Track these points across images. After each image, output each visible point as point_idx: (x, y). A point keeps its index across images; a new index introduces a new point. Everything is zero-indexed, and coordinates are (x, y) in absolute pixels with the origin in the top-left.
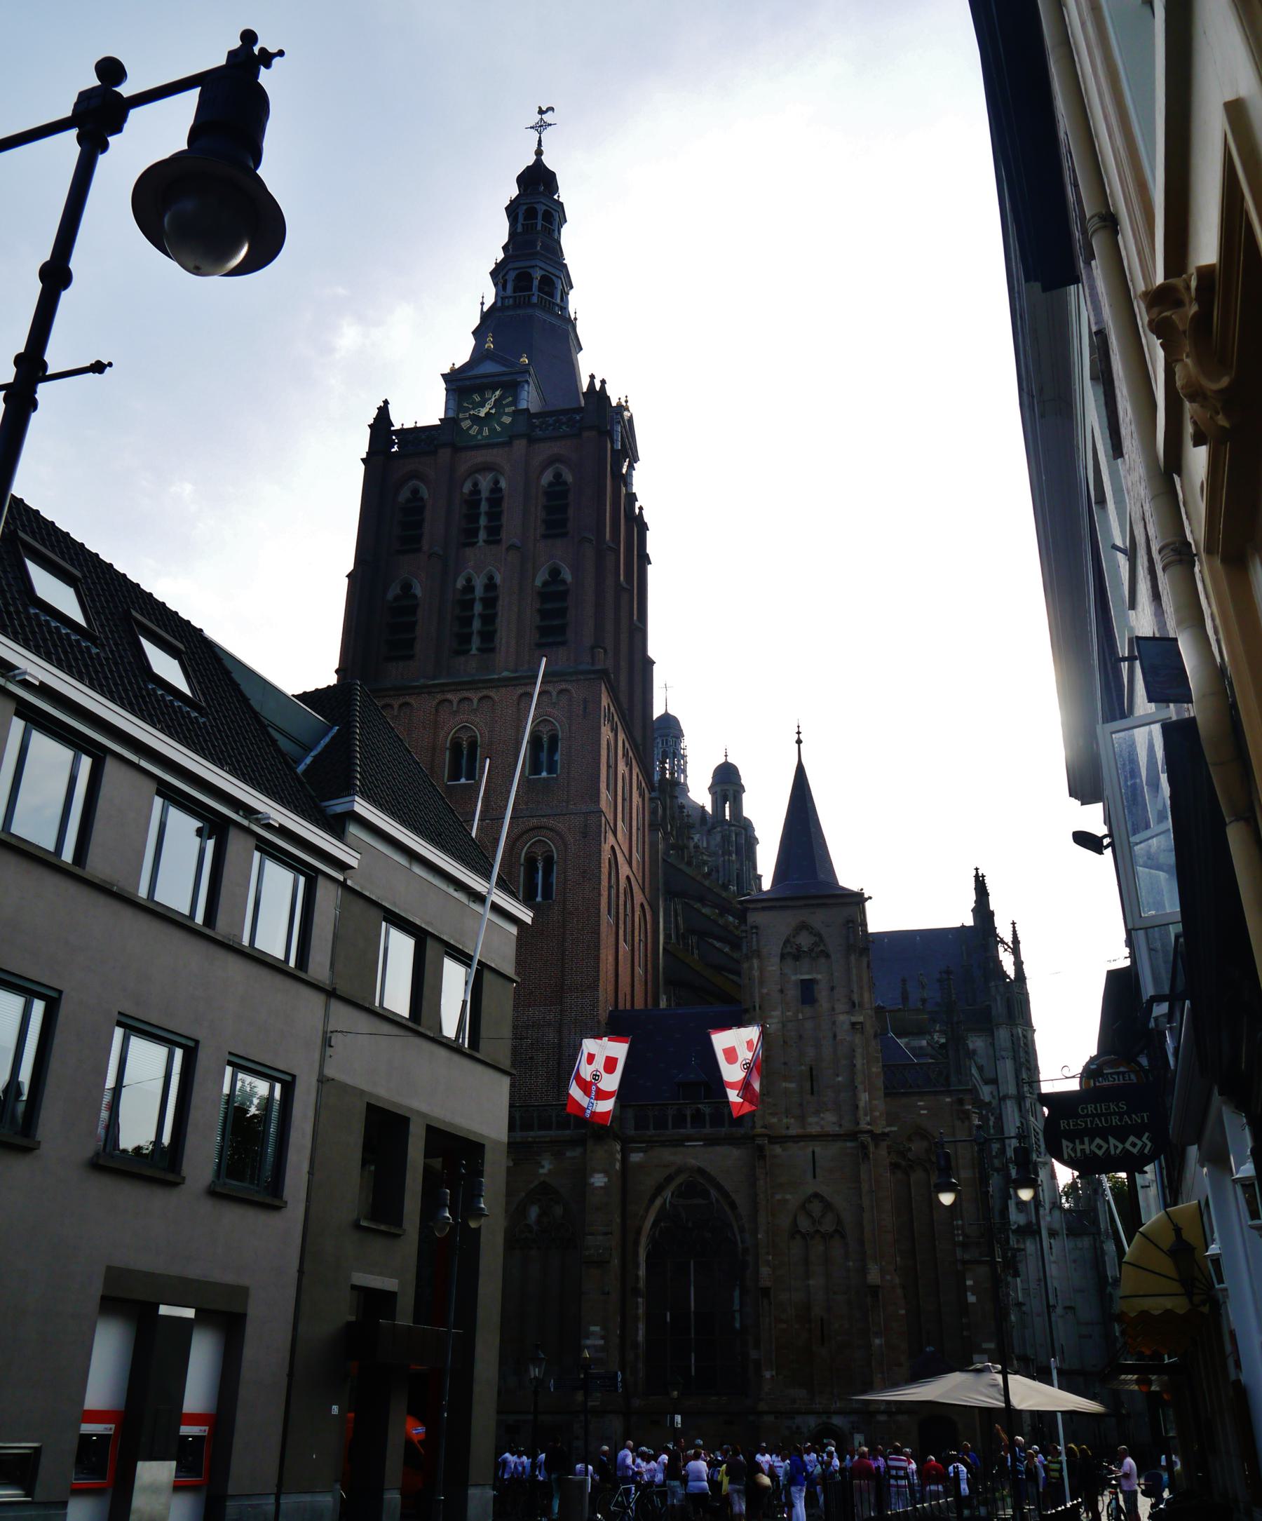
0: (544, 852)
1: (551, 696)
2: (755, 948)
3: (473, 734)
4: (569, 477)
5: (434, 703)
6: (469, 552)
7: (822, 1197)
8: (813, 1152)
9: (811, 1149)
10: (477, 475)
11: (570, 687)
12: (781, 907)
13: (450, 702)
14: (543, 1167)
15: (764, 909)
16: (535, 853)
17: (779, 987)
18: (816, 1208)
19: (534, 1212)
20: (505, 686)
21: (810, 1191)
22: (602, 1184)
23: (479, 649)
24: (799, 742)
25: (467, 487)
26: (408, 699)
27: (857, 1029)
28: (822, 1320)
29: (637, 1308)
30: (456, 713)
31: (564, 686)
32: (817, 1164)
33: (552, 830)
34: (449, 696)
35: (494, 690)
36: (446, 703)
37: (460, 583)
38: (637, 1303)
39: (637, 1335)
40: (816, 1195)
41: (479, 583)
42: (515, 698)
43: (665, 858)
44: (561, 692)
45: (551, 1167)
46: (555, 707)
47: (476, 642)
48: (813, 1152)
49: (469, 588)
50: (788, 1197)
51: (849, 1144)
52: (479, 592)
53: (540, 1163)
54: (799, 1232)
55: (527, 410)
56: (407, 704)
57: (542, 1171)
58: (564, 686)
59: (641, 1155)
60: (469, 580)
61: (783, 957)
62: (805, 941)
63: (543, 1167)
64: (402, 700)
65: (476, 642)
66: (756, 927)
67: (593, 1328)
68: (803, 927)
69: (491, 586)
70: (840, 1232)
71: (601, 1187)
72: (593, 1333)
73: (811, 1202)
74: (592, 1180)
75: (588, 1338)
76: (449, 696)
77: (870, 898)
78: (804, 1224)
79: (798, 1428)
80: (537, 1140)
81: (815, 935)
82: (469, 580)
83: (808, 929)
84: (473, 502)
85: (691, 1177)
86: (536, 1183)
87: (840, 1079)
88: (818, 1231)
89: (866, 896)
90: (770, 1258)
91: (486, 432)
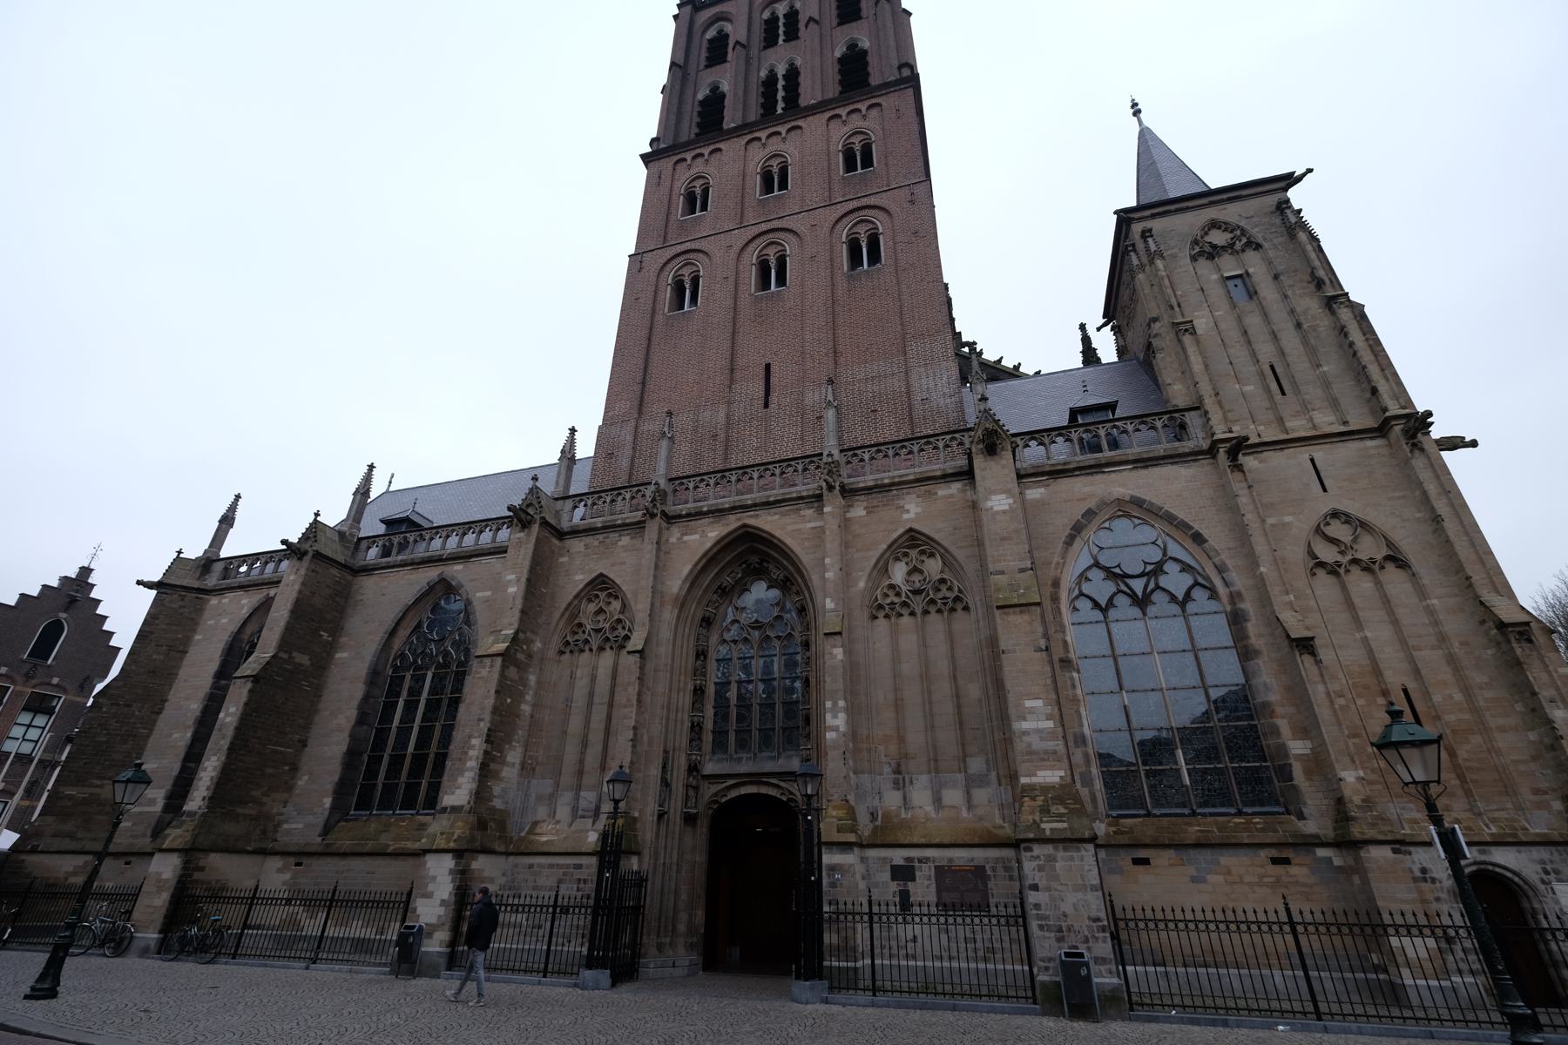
5: (744, 143)
6: (770, 51)
7: (1346, 515)
8: (1312, 460)
9: (1307, 456)
12: (1177, 211)
13: (759, 139)
16: (857, 233)
17: (1197, 286)
18: (1338, 530)
19: (899, 573)
20: (812, 115)
21: (1325, 509)
22: (1007, 507)
23: (784, 41)
24: (1137, 113)
26: (717, 146)
27: (1342, 303)
28: (1405, 691)
29: (1074, 686)
30: (764, 145)
32: (1322, 475)
37: (763, 73)
38: (1072, 679)
40: (1335, 514)
41: (781, 70)
42: (824, 121)
44: (870, 107)
45: (919, 510)
48: (1312, 460)
50: (1288, 519)
54: (1321, 564)
56: (719, 150)
57: (905, 516)
59: (1042, 490)
60: (771, 71)
61: (1194, 258)
62: (1219, 238)
63: (908, 511)
70: (1396, 559)
71: (1004, 512)
72: (1032, 711)
73: (1328, 524)
74: (989, 504)
75: (1025, 719)
78: (1327, 554)
79: (1424, 871)
80: (896, 480)
82: (771, 71)
83: (1219, 228)
85: (1119, 510)
86: (901, 531)
88: (1355, 561)
90: (1292, 597)
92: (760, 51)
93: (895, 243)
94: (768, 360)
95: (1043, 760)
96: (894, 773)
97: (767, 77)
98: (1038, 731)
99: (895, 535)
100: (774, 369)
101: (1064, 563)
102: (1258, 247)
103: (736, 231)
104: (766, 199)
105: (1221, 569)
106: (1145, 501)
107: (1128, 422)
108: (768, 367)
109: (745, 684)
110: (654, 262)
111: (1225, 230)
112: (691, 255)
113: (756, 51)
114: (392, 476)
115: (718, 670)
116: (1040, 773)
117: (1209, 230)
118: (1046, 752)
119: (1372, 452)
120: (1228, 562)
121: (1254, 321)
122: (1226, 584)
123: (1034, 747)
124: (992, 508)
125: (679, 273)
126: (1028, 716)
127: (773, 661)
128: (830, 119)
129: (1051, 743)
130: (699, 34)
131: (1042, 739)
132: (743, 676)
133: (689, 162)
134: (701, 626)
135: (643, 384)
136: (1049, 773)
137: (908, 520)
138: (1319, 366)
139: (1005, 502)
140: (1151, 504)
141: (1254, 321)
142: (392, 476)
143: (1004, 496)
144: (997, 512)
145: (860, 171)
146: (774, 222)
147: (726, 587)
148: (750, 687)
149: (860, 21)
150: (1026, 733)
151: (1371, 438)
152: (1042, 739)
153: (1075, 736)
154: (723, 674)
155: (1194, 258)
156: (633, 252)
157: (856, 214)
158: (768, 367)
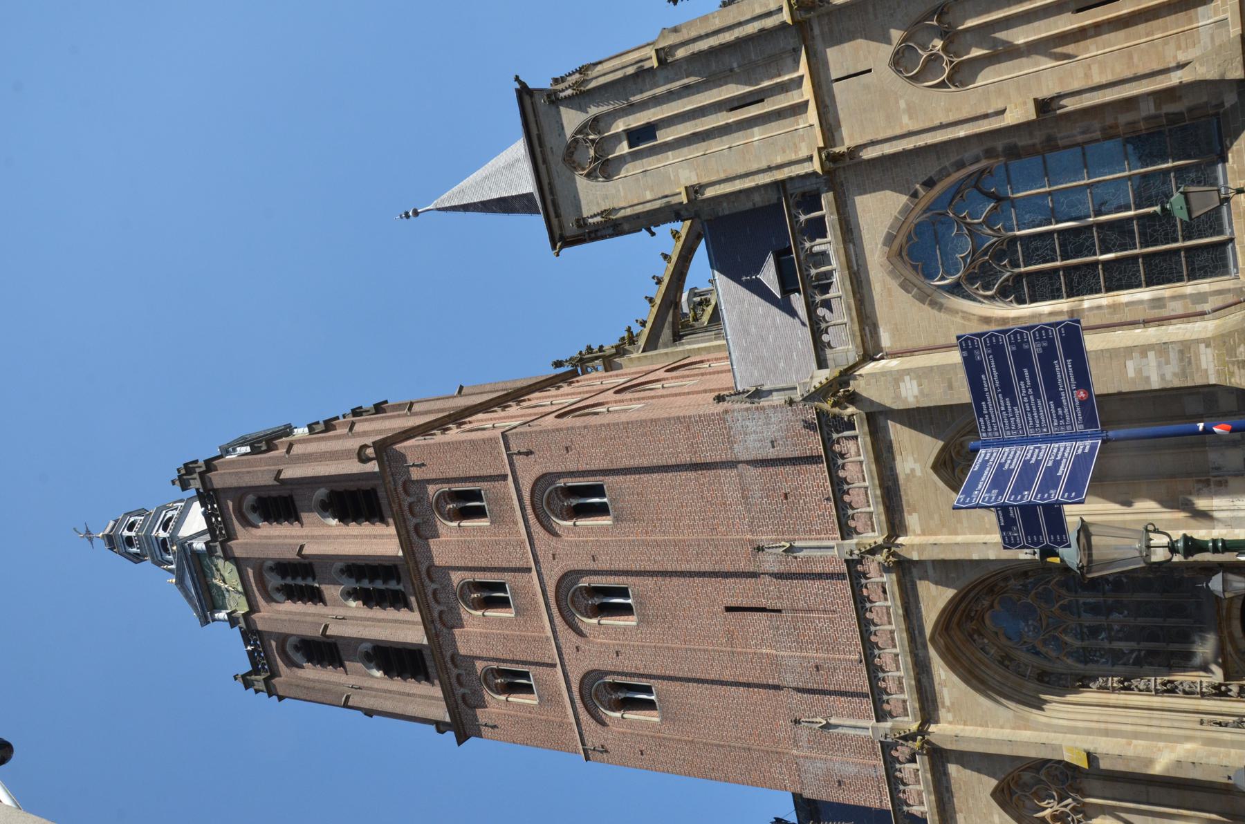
0: (559, 498)
1: (413, 502)
3: (466, 587)
10: (269, 589)
11: (400, 483)
12: (552, 193)
13: (441, 613)
14: (913, 470)
15: (558, 215)
21: (890, 74)
22: (915, 383)
26: (448, 659)
29: (1099, 307)
32: (852, 72)
34: (436, 614)
35: (420, 566)
36: (445, 618)
38: (1091, 309)
39: (1141, 302)
43: (641, 350)
45: (910, 459)
46: (422, 498)
51: (817, 31)
53: (908, 476)
57: (918, 473)
63: (913, 470)
65: (393, 585)
67: (1131, 373)
71: (920, 385)
72: (1139, 371)
75: (1148, 378)
76: (436, 614)
83: (572, 153)
87: (735, 65)
94: (721, 609)
95: (1190, 363)
96: (1209, 485)
97: (356, 599)
98: (1159, 366)
99: (941, 484)
100: (733, 602)
101: (963, 312)
105: (960, 165)
106: (888, 233)
107: (800, 247)
108: (729, 609)
109: (1113, 633)
115: (1097, 662)
116: (1204, 366)
117: (574, 162)
118: (1181, 360)
119: (826, 29)
120: (953, 160)
122: (977, 160)
123: (1177, 370)
124: (916, 397)
126: (1145, 374)
127: (1084, 604)
129: (1172, 355)
131: (1168, 363)
132: (1103, 635)
133: (466, 691)
134: (1048, 683)
136: (1203, 358)
137: (922, 471)
138: (731, 70)
139: (908, 386)
140: (891, 227)
143: (902, 385)
144: (921, 392)
145: (484, 503)
147: (1001, 657)
148: (1116, 627)
149: (295, 497)
150: (1163, 377)
151: (812, 30)
152: (1168, 363)
153: (1154, 308)
154: (1102, 656)
158: (729, 609)
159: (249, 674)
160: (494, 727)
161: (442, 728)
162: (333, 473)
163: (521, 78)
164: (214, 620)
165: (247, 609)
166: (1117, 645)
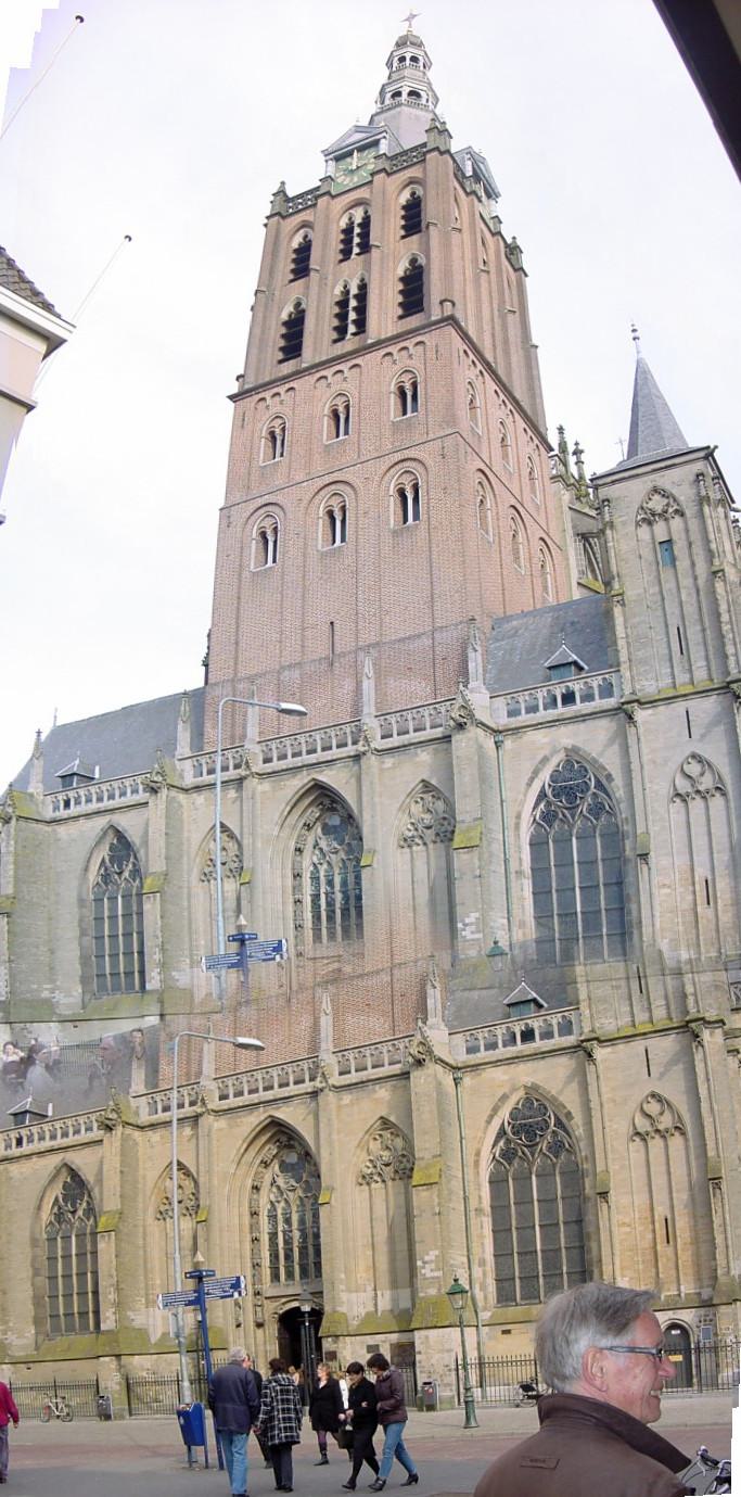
2: (607, 519)
4: (420, 192)
15: (613, 482)
25: (343, 223)
31: (419, 339)
33: (415, 460)
36: (323, 381)
37: (338, 290)
47: (352, 329)
49: (346, 292)
52: (354, 291)
55: (385, 154)
58: (419, 339)
61: (637, 524)
62: (657, 503)
64: (287, 386)
65: (352, 329)
66: (608, 500)
68: (656, 490)
69: (363, 287)
77: (716, 447)
81: (668, 497)
84: (348, 231)
89: (712, 447)
91: (356, 179)
92: (335, 266)
93: (428, 499)
100: (337, 627)
102: (682, 515)
103: (305, 484)
104: (330, 445)
110: (239, 515)
111: (663, 496)
112: (269, 508)
113: (332, 266)
114: (56, 710)
121: (669, 585)
125: (262, 525)
128: (385, 356)
130: (287, 239)
135: (237, 643)
141: (669, 585)
142: (56, 710)
146: (335, 474)
155: (637, 524)
156: (222, 504)
157: (400, 465)
159: (285, 195)
160: (243, 426)
161: (241, 380)
162: (432, 276)
163: (716, 451)
164: (326, 161)
165: (333, 193)
166: (323, 897)
